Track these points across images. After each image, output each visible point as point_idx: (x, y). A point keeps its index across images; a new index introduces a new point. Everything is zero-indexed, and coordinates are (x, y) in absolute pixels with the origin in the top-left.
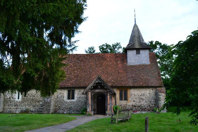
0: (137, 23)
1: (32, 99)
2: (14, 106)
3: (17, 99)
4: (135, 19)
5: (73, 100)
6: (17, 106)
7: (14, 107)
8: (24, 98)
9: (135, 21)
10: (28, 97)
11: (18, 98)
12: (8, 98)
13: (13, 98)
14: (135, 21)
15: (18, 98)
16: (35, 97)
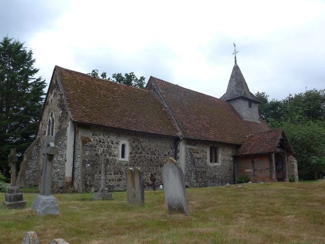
0: (238, 63)
1: (151, 160)
2: (114, 174)
3: (121, 159)
4: (235, 57)
5: (217, 164)
6: (121, 173)
7: (113, 176)
8: (135, 156)
9: (236, 61)
10: (143, 154)
11: (123, 156)
12: (99, 153)
13: (110, 154)
14: (236, 61)
15: (123, 156)
16: (155, 154)
